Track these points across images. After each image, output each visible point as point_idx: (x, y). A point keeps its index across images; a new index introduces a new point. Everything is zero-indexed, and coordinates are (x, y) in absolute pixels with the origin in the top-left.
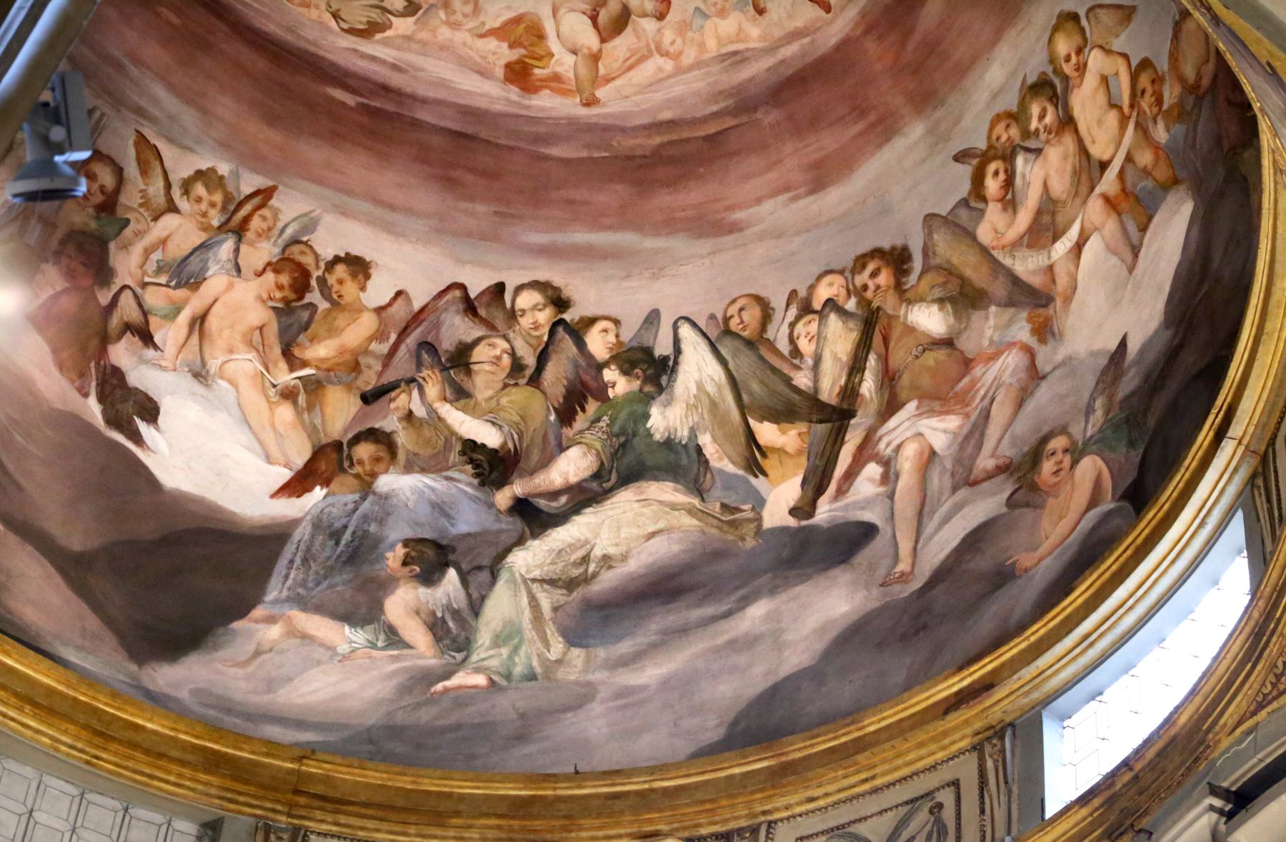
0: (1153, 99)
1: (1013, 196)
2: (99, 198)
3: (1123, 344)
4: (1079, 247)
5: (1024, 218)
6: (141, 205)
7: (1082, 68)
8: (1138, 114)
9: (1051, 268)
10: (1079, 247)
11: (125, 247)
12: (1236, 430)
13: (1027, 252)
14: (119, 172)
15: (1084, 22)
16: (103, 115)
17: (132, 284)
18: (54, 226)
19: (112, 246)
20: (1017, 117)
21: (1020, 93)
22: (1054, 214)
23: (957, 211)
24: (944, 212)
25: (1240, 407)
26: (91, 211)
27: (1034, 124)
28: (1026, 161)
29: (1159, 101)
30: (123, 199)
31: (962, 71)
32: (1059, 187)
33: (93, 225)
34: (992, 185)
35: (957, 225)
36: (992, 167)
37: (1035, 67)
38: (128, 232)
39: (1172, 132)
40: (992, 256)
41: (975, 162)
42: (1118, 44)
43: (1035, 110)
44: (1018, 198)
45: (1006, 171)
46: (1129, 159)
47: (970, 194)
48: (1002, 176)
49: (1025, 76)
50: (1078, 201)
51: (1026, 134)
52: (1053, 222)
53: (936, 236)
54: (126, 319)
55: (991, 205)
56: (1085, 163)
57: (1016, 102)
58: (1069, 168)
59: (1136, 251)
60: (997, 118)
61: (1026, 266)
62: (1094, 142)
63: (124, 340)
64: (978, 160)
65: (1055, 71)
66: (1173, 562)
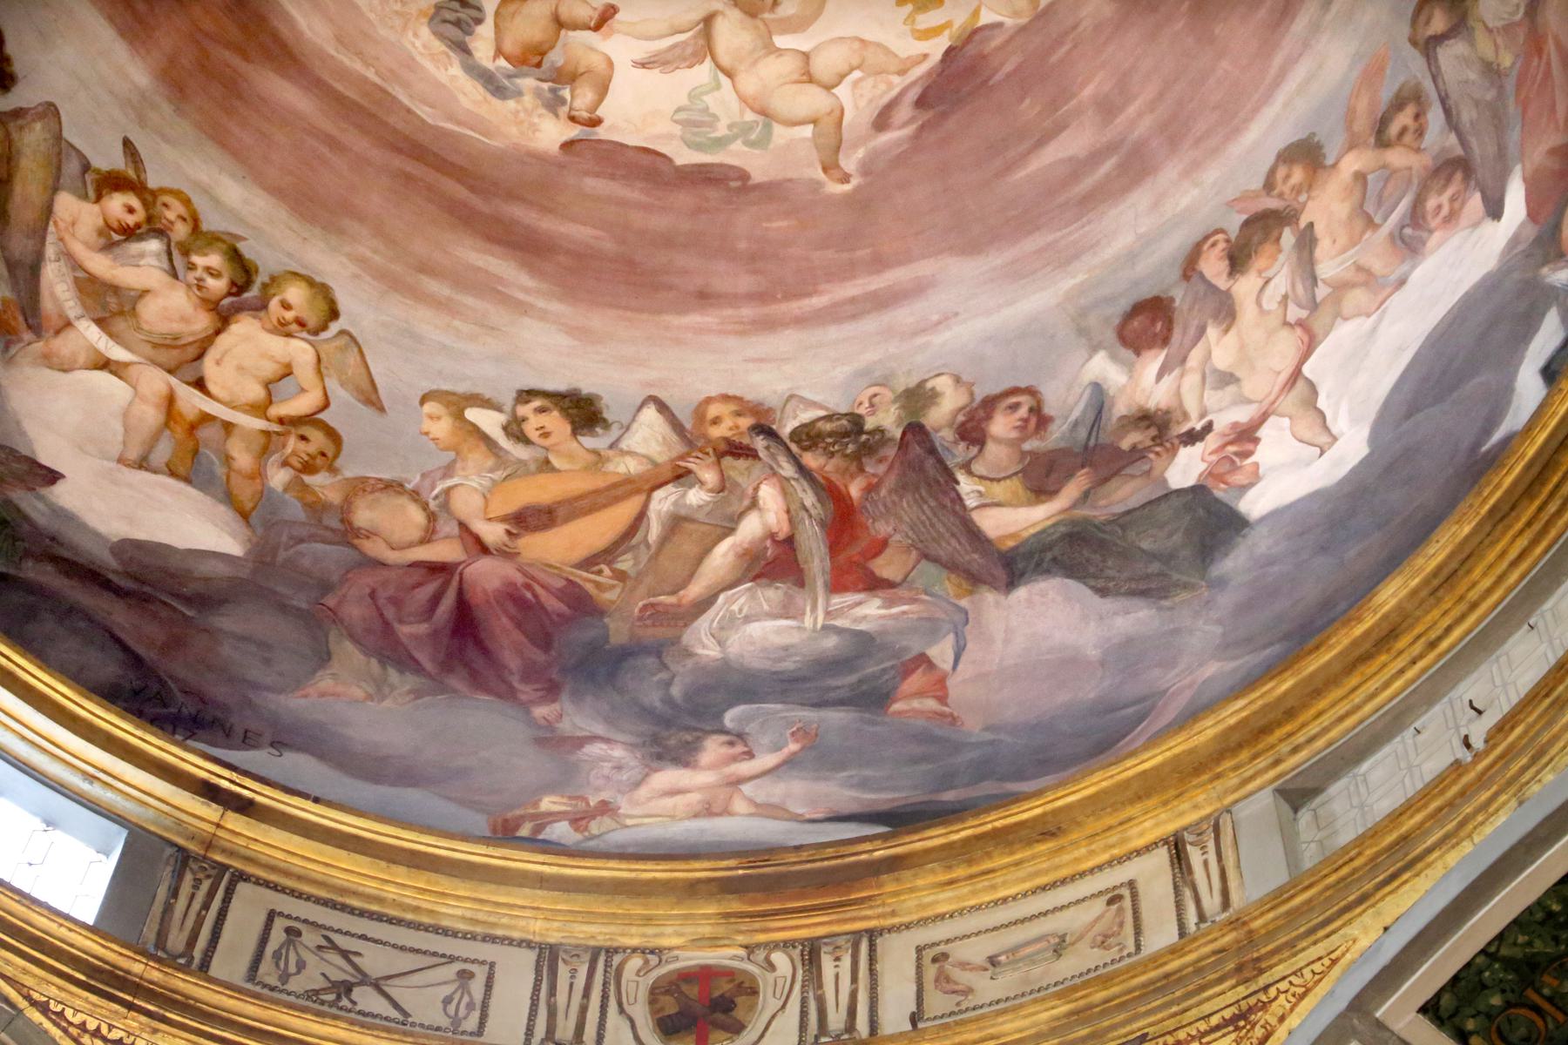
0: (306, 458)
1: (117, 244)
3: (53, 477)
4: (105, 365)
5: (100, 265)
7: (282, 329)
8: (277, 433)
9: (68, 324)
10: (105, 365)
12: (235, 822)
13: (70, 280)
15: (334, 327)
20: (200, 237)
21: (223, 233)
22: (121, 313)
23: (74, 153)
24: (65, 134)
25: (273, 829)
27: (197, 260)
28: (158, 255)
29: (308, 468)
31: (220, 138)
32: (150, 311)
34: (117, 204)
35: (59, 154)
36: (135, 202)
37: (265, 256)
39: (287, 496)
40: (47, 224)
41: (131, 173)
42: (332, 384)
43: (214, 260)
44: (117, 251)
45: (138, 226)
46: (228, 427)
47: (98, 171)
48: (131, 220)
49: (245, 239)
50: (148, 349)
51: (186, 253)
52: (114, 315)
53: (38, 126)
55: (96, 208)
56: (192, 352)
57: (213, 227)
58: (176, 327)
59: (142, 464)
60: (187, 202)
61: (57, 286)
62: (218, 363)
64: (135, 177)
65: (265, 286)
66: (24, 738)
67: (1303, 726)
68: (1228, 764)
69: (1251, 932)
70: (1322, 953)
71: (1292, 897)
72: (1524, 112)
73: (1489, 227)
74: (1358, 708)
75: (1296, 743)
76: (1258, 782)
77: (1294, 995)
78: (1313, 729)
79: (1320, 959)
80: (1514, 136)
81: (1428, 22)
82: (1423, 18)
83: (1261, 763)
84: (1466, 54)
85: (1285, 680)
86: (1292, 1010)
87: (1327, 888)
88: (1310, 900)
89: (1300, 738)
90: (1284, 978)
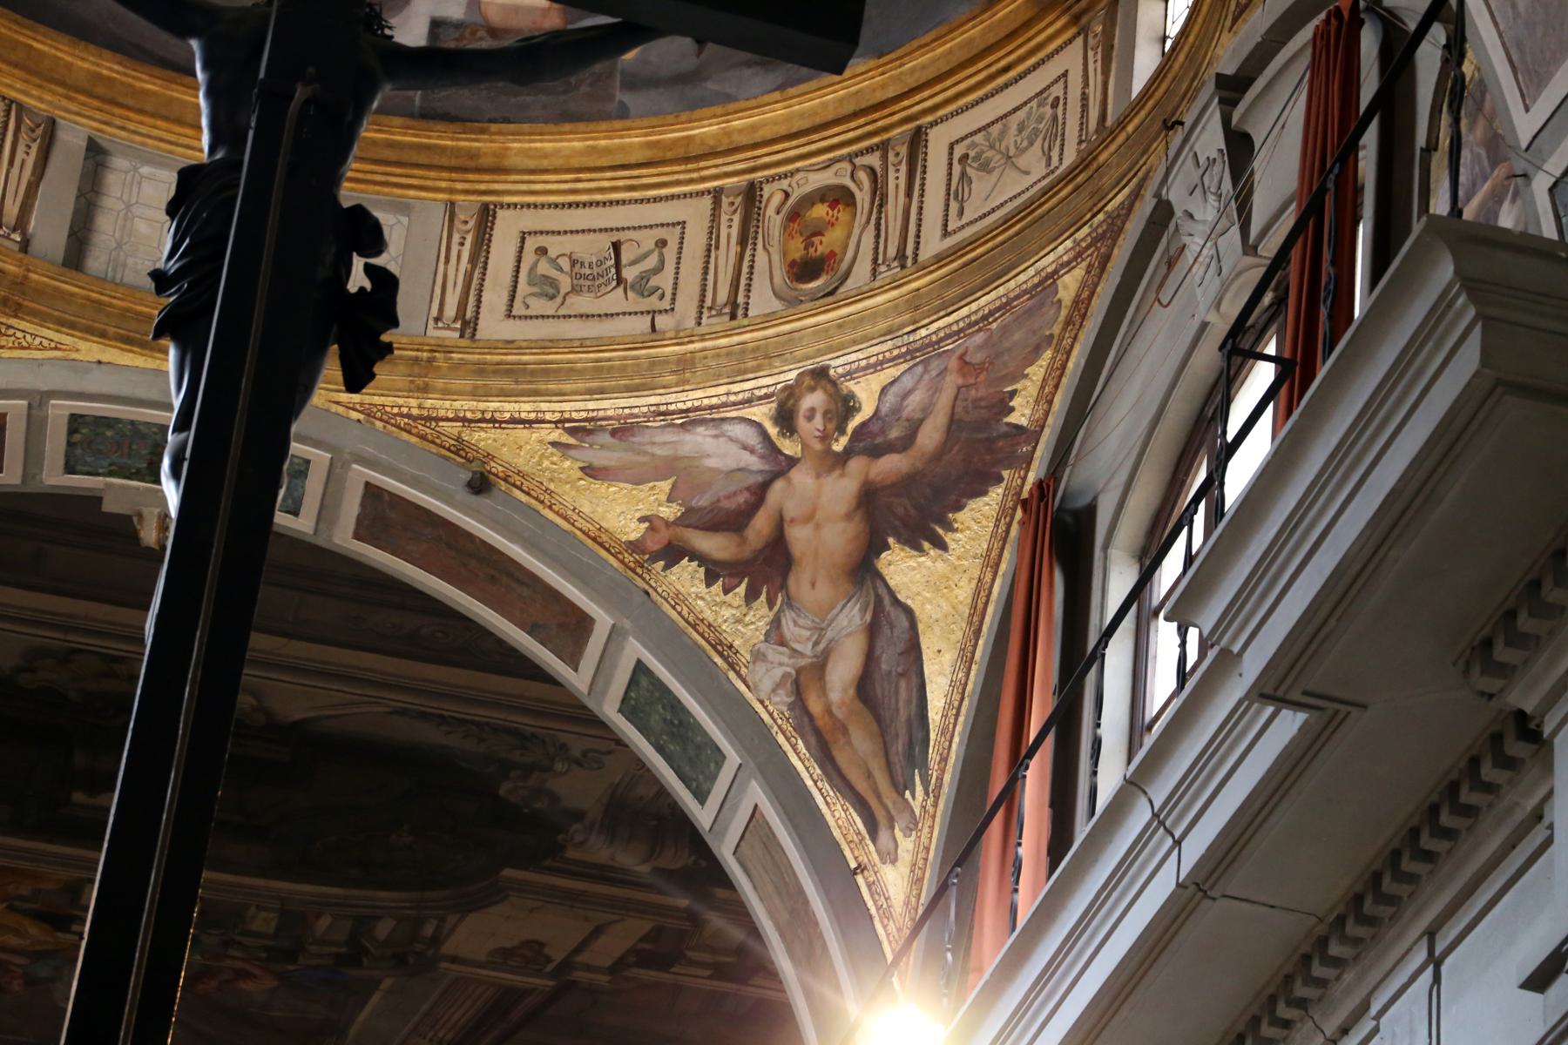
67: (142, 123)
68: (81, 98)
69: (26, 277)
70: (56, 339)
71: (66, 283)
74: (177, 144)
75: (127, 126)
76: (84, 121)
77: (19, 343)
78: (144, 130)
79: (52, 341)
83: (98, 115)
85: (154, 84)
86: (10, 348)
87: (87, 298)
88: (72, 295)
89: (132, 126)
90: (24, 331)
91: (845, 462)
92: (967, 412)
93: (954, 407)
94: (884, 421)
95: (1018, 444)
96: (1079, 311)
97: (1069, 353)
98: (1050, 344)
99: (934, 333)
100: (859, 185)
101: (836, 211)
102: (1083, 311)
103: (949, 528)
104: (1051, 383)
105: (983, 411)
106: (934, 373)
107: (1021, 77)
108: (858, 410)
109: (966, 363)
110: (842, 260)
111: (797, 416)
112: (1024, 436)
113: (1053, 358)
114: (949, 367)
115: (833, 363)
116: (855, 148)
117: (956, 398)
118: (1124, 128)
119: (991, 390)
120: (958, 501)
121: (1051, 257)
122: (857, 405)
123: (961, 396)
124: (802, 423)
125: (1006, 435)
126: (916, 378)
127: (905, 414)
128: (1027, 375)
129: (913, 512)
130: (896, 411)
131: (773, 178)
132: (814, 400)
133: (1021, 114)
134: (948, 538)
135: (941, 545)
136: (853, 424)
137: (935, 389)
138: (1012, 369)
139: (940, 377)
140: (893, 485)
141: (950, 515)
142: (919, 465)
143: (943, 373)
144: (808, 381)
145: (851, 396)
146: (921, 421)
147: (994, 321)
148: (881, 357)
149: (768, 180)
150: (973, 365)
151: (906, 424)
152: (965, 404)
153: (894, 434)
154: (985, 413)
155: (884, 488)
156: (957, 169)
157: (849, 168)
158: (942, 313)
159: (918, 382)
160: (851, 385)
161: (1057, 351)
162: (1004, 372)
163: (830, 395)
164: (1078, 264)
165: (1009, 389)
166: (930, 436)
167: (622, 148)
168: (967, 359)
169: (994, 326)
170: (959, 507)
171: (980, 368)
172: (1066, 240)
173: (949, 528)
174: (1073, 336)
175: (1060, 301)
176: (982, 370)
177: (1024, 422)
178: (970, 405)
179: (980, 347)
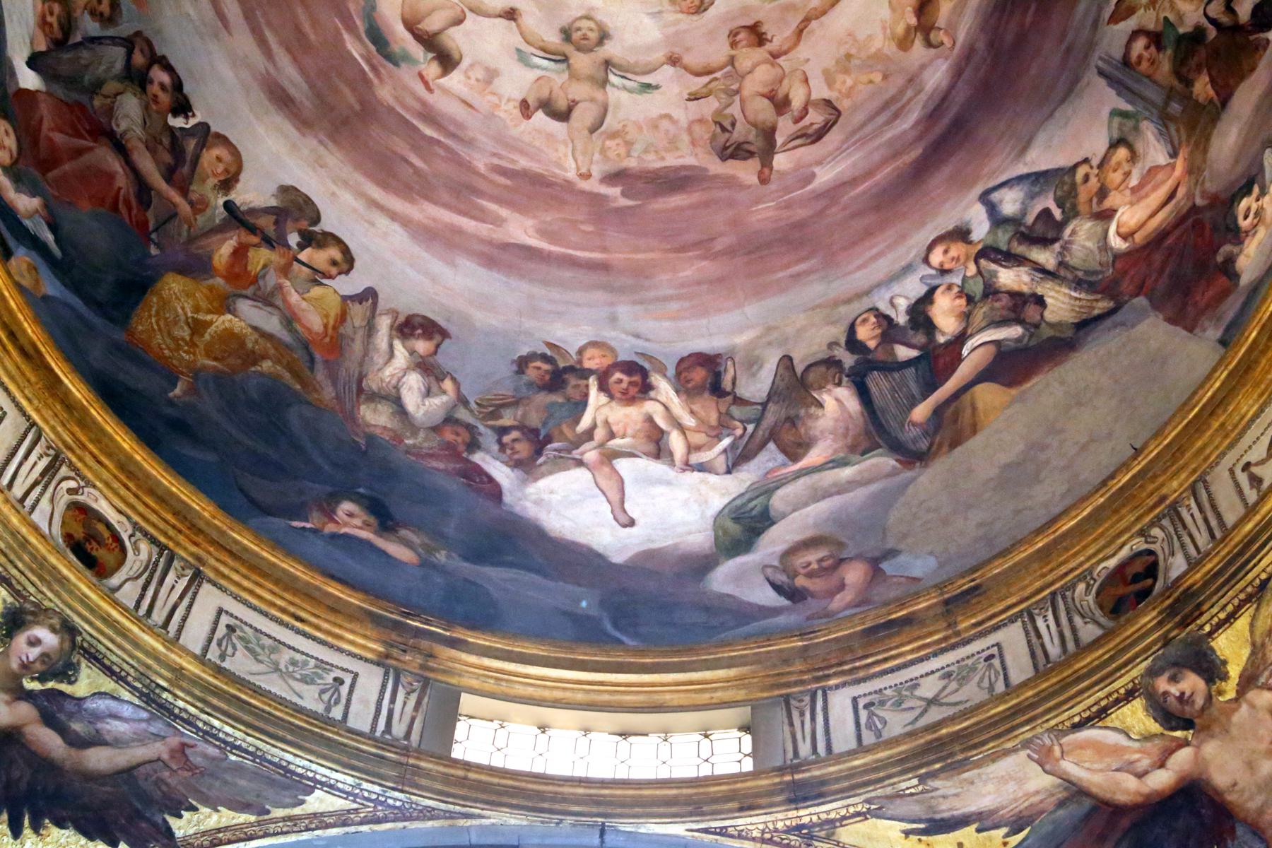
2: (1153, 49)
6: (1154, 9)
11: (1180, 17)
14: (1135, 34)
16: (1101, 58)
17: (1202, 8)
18: (1172, 88)
19: (1181, 30)
26: (1161, 56)
30: (1151, 26)
33: (1169, 52)
38: (1172, 17)
54: (1223, 9)
63: (1236, 9)
72: (67, 104)
73: (26, 54)
80: (60, 92)
81: (142, 51)
82: (146, 48)
84: (113, 70)
91: (19, 699)
92: (146, 780)
93: (139, 765)
94: (80, 711)
95: (157, 841)
96: (311, 823)
97: (266, 835)
98: (259, 814)
99: (180, 709)
100: (137, 550)
101: (114, 545)
102: (313, 826)
103: (36, 828)
104: (229, 835)
105: (158, 792)
106: (152, 729)
107: (305, 634)
108: (71, 683)
109: (183, 752)
110: (106, 577)
111: (24, 631)
112: (165, 841)
113: (251, 824)
114: (168, 740)
115: (84, 634)
116: (143, 524)
117: (150, 762)
118: (468, 770)
119: (181, 788)
120: (64, 820)
121: (327, 772)
122: (73, 679)
123: (155, 766)
124: (21, 640)
125: (155, 825)
126: (135, 716)
127: (99, 725)
128: (218, 811)
129: (23, 786)
130: (97, 717)
131: (76, 470)
132: (49, 639)
133: (298, 657)
134: (27, 831)
135: (16, 832)
136: (51, 685)
137: (141, 739)
138: (210, 794)
139: (152, 737)
140: (34, 754)
141: (47, 821)
142: (68, 765)
143: (158, 737)
144: (55, 621)
145: (75, 668)
146: (105, 743)
147: (235, 754)
148: (123, 674)
149: (71, 466)
150: (188, 760)
151: (94, 732)
152: (151, 772)
153: (77, 726)
154: (157, 795)
155: (24, 746)
156: (221, 630)
157: (130, 532)
158: (199, 704)
159: (134, 720)
160: (84, 663)
161: (259, 823)
162: (205, 790)
163: (62, 649)
164: (346, 799)
165: (194, 803)
166: (98, 759)
167: (19, 324)
168: (188, 751)
169: (233, 758)
170: (60, 824)
171: (189, 766)
172: (353, 776)
173: (36, 828)
174: (285, 829)
175: (302, 802)
176: (190, 770)
177: (179, 834)
178: (154, 778)
179: (205, 756)
